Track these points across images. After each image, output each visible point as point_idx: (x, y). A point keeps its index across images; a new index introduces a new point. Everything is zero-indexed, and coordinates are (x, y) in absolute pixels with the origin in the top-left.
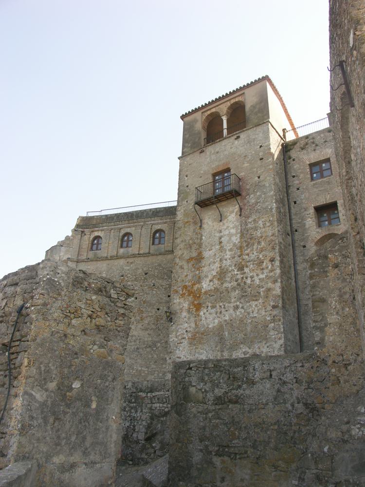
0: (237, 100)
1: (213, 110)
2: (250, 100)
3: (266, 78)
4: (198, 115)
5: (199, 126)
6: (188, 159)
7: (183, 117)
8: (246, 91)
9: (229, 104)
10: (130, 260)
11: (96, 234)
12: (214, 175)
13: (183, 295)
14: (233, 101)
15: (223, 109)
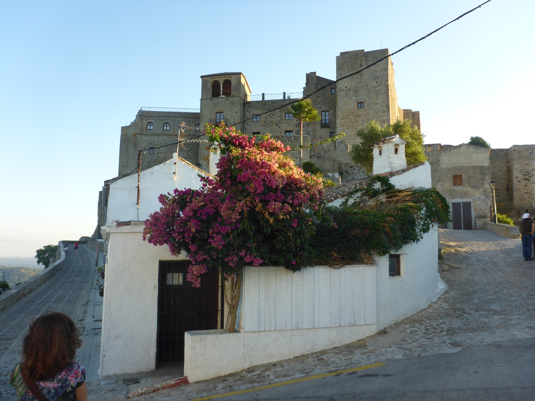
0: (228, 78)
1: (217, 79)
2: (233, 83)
3: (240, 73)
4: (209, 79)
5: (210, 86)
6: (205, 101)
7: (202, 77)
8: (233, 76)
9: (224, 79)
10: (169, 137)
11: (150, 121)
12: (217, 113)
13: (203, 160)
14: (226, 78)
15: (221, 81)
